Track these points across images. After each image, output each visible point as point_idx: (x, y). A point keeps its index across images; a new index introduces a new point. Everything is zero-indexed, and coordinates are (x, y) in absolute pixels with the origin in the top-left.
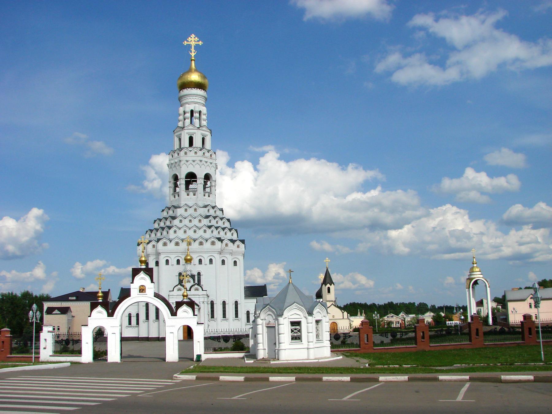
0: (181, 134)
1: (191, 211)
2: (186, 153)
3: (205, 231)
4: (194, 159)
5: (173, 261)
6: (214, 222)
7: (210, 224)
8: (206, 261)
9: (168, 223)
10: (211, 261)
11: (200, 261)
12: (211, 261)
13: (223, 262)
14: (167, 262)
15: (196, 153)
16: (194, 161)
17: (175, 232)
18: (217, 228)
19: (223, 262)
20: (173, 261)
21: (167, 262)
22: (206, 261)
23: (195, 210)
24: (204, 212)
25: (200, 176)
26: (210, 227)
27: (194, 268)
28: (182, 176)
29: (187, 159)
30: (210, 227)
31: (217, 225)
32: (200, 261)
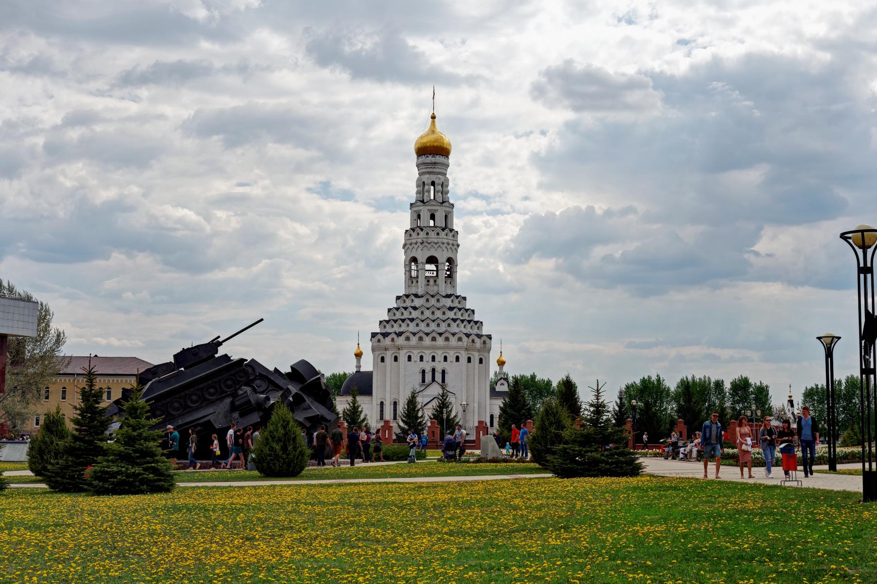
1: (433, 301)
6: (459, 316)
7: (455, 317)
8: (451, 357)
9: (406, 315)
10: (457, 359)
11: (445, 359)
12: (457, 359)
13: (469, 360)
14: (409, 358)
15: (438, 234)
17: (417, 325)
18: (463, 321)
19: (469, 360)
21: (409, 358)
22: (451, 357)
23: (438, 300)
24: (448, 302)
26: (454, 320)
27: (439, 366)
28: (422, 257)
30: (454, 320)
31: (462, 318)
32: (445, 359)
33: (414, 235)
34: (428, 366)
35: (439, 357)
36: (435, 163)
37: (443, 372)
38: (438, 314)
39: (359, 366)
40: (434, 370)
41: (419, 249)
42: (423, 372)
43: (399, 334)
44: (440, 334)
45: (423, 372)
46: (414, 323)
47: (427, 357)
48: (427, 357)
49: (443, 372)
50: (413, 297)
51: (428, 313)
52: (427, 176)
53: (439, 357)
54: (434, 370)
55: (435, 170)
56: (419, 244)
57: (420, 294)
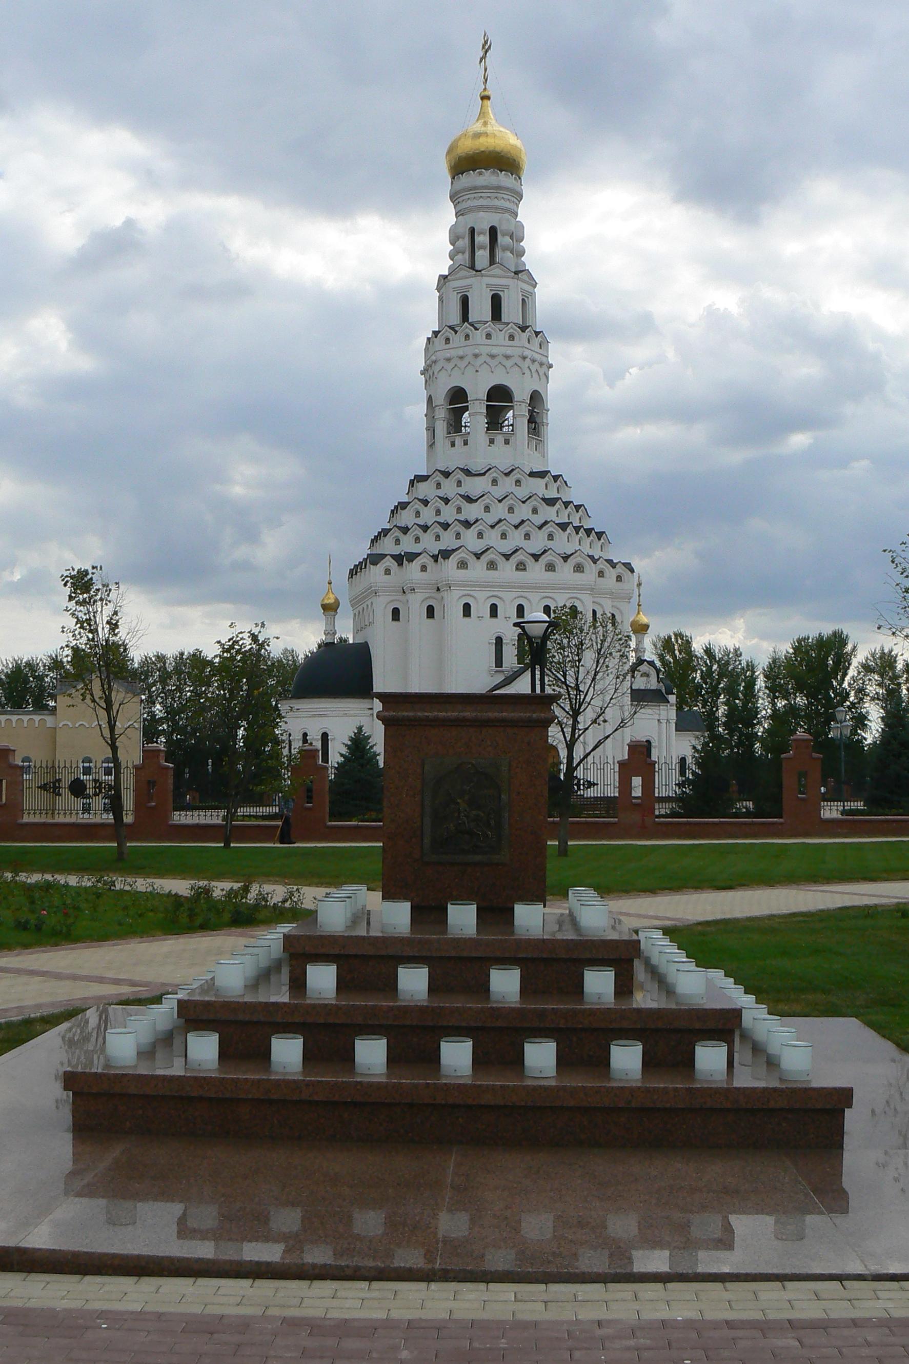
0: (470, 286)
1: (507, 485)
2: (489, 336)
3: (551, 537)
4: (509, 352)
5: (481, 608)
14: (467, 610)
15: (512, 337)
16: (507, 357)
20: (481, 608)
21: (467, 610)
25: (521, 394)
29: (495, 351)
33: (457, 339)
36: (499, 188)
38: (524, 512)
39: (330, 632)
41: (470, 371)
42: (499, 641)
43: (446, 554)
44: (536, 557)
45: (499, 641)
46: (474, 530)
50: (461, 475)
51: (500, 511)
55: (497, 203)
56: (469, 358)
57: (474, 469)
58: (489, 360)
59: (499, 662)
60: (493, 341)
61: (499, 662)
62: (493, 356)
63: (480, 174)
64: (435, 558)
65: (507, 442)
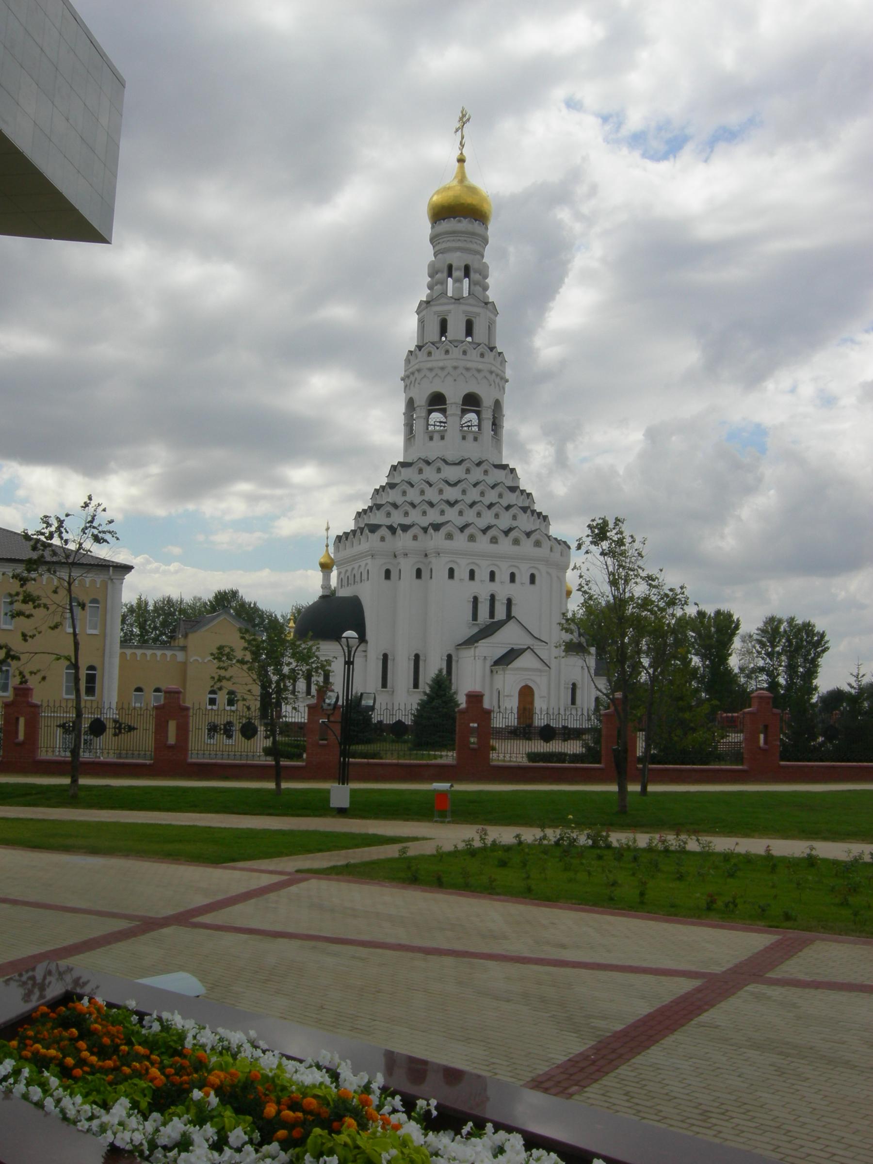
0: (449, 312)
4: (480, 367)
5: (462, 573)
8: (523, 577)
14: (451, 573)
16: (479, 371)
20: (462, 573)
21: (451, 573)
22: (523, 577)
25: (487, 402)
27: (503, 590)
34: (482, 588)
35: (503, 576)
37: (509, 602)
40: (493, 598)
42: (475, 600)
43: (437, 527)
45: (475, 600)
47: (482, 574)
48: (482, 574)
49: (509, 602)
52: (458, 254)
53: (503, 576)
54: (493, 598)
58: (464, 372)
59: (475, 617)
60: (468, 357)
61: (475, 617)
62: (468, 369)
63: (460, 221)
64: (425, 530)
65: (476, 439)
